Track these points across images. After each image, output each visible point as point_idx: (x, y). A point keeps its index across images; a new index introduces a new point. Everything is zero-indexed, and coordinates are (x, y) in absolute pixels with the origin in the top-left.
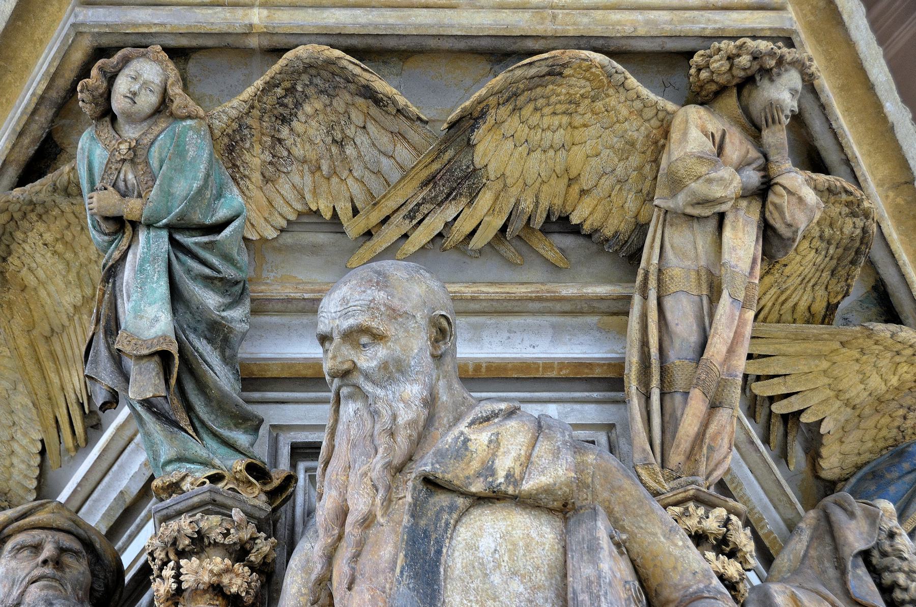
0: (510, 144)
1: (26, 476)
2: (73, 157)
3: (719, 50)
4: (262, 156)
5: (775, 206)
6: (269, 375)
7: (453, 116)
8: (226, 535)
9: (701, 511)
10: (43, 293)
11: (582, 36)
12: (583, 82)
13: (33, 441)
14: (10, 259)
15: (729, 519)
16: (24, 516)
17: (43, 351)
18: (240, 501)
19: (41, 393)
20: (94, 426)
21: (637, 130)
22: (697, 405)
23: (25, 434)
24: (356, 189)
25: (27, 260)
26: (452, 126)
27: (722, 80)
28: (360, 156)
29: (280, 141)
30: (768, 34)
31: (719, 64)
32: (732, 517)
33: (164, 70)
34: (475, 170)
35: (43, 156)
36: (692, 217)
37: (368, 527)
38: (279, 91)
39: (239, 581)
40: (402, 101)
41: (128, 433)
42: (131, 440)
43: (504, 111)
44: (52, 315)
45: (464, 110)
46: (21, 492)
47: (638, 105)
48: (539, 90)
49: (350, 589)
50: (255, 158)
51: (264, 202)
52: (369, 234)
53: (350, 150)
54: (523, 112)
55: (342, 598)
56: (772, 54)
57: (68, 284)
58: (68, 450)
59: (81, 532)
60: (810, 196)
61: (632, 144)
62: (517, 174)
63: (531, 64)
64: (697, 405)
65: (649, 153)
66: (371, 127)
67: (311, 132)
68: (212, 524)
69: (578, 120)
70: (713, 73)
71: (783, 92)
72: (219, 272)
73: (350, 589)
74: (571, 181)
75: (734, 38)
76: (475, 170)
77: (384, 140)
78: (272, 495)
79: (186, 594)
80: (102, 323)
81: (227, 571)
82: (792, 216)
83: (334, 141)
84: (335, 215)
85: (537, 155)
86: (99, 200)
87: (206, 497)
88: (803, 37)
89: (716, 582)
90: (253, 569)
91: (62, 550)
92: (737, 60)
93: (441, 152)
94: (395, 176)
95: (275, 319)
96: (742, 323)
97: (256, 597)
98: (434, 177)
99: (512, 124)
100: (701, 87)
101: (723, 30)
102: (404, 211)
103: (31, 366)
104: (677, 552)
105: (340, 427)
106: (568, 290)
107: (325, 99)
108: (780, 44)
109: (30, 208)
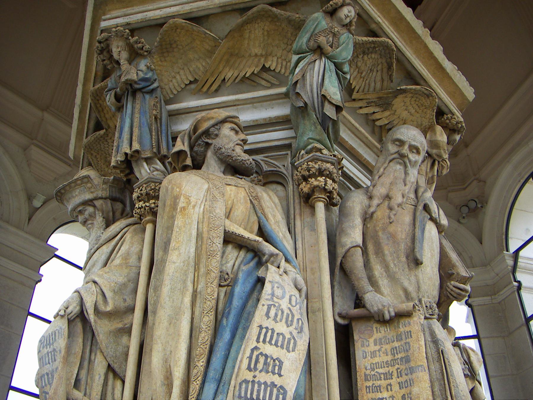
0: (403, 104)
3: (455, 119)
10: (246, 42)
12: (429, 103)
17: (225, 58)
26: (401, 89)
29: (357, 57)
33: (355, 16)
38: (373, 45)
43: (411, 95)
46: (169, 92)
52: (354, 100)
61: (422, 125)
67: (368, 62)
70: (450, 122)
73: (391, 223)
77: (379, 78)
85: (406, 112)
86: (322, 40)
93: (390, 93)
99: (407, 100)
102: (368, 101)
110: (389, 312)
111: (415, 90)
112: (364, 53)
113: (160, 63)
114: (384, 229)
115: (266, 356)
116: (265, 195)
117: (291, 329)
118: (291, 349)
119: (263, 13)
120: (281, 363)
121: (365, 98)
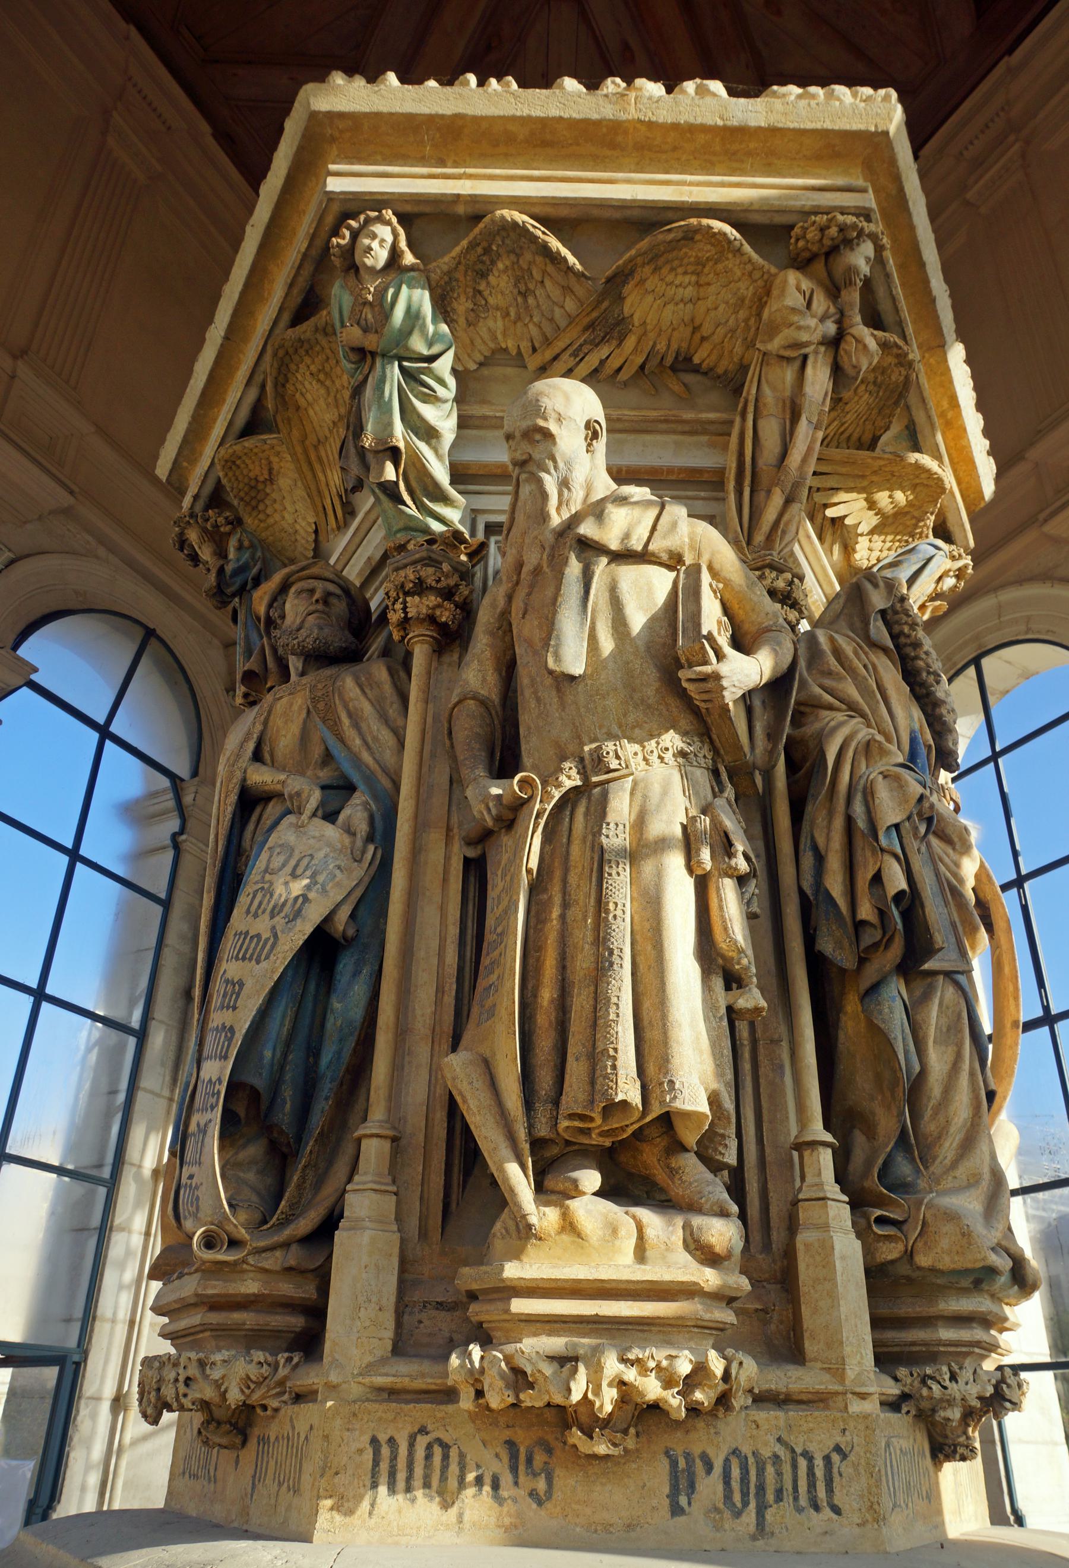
0: (650, 298)
1: (306, 549)
2: (329, 304)
4: (467, 305)
5: (845, 351)
6: (470, 472)
7: (609, 273)
8: (438, 581)
9: (774, 574)
10: (311, 412)
11: (710, 209)
12: (709, 247)
13: (309, 524)
14: (288, 386)
15: (792, 581)
16: (303, 569)
17: (313, 457)
18: (448, 558)
19: (313, 487)
20: (350, 511)
21: (746, 289)
22: (777, 499)
23: (304, 519)
24: (534, 331)
25: (299, 387)
26: (609, 280)
27: (815, 248)
28: (538, 306)
29: (480, 292)
30: (853, 211)
31: (812, 234)
32: (795, 580)
34: (623, 319)
35: (307, 305)
36: (782, 358)
37: (537, 575)
39: (447, 613)
40: (572, 259)
41: (372, 516)
42: (375, 522)
43: (647, 270)
44: (318, 428)
45: (618, 267)
47: (749, 267)
48: (675, 254)
49: (523, 618)
50: (462, 306)
51: (468, 342)
53: (531, 301)
54: (663, 271)
55: (518, 625)
56: (854, 226)
57: (328, 405)
58: (333, 530)
59: (341, 582)
60: (872, 344)
61: (742, 300)
62: (655, 322)
63: (670, 230)
64: (777, 499)
65: (754, 308)
66: (548, 283)
67: (503, 284)
68: (428, 573)
69: (703, 279)
70: (808, 242)
71: (861, 258)
72: (435, 392)
73: (523, 618)
74: (696, 329)
75: (827, 214)
76: (623, 319)
77: (556, 293)
78: (470, 556)
79: (411, 622)
80: (351, 429)
81: (439, 606)
82: (857, 359)
83: (520, 293)
84: (519, 353)
85: (670, 307)
87: (424, 554)
88: (877, 215)
89: (781, 620)
90: (457, 606)
91: (329, 594)
92: (827, 232)
93: (599, 302)
94: (563, 323)
95: (474, 432)
96: (813, 441)
97: (460, 626)
98: (593, 323)
100: (798, 254)
101: (819, 206)
102: (570, 351)
103: (305, 468)
104: (755, 599)
105: (519, 504)
106: (689, 415)
107: (513, 257)
108: (862, 219)
109: (299, 345)
110: (489, 810)
111: (640, 254)
112: (483, 275)
113: (262, 525)
114: (519, 636)
115: (227, 981)
116: (349, 683)
117: (277, 919)
118: (263, 957)
119: (281, 353)
120: (241, 984)
121: (557, 350)
